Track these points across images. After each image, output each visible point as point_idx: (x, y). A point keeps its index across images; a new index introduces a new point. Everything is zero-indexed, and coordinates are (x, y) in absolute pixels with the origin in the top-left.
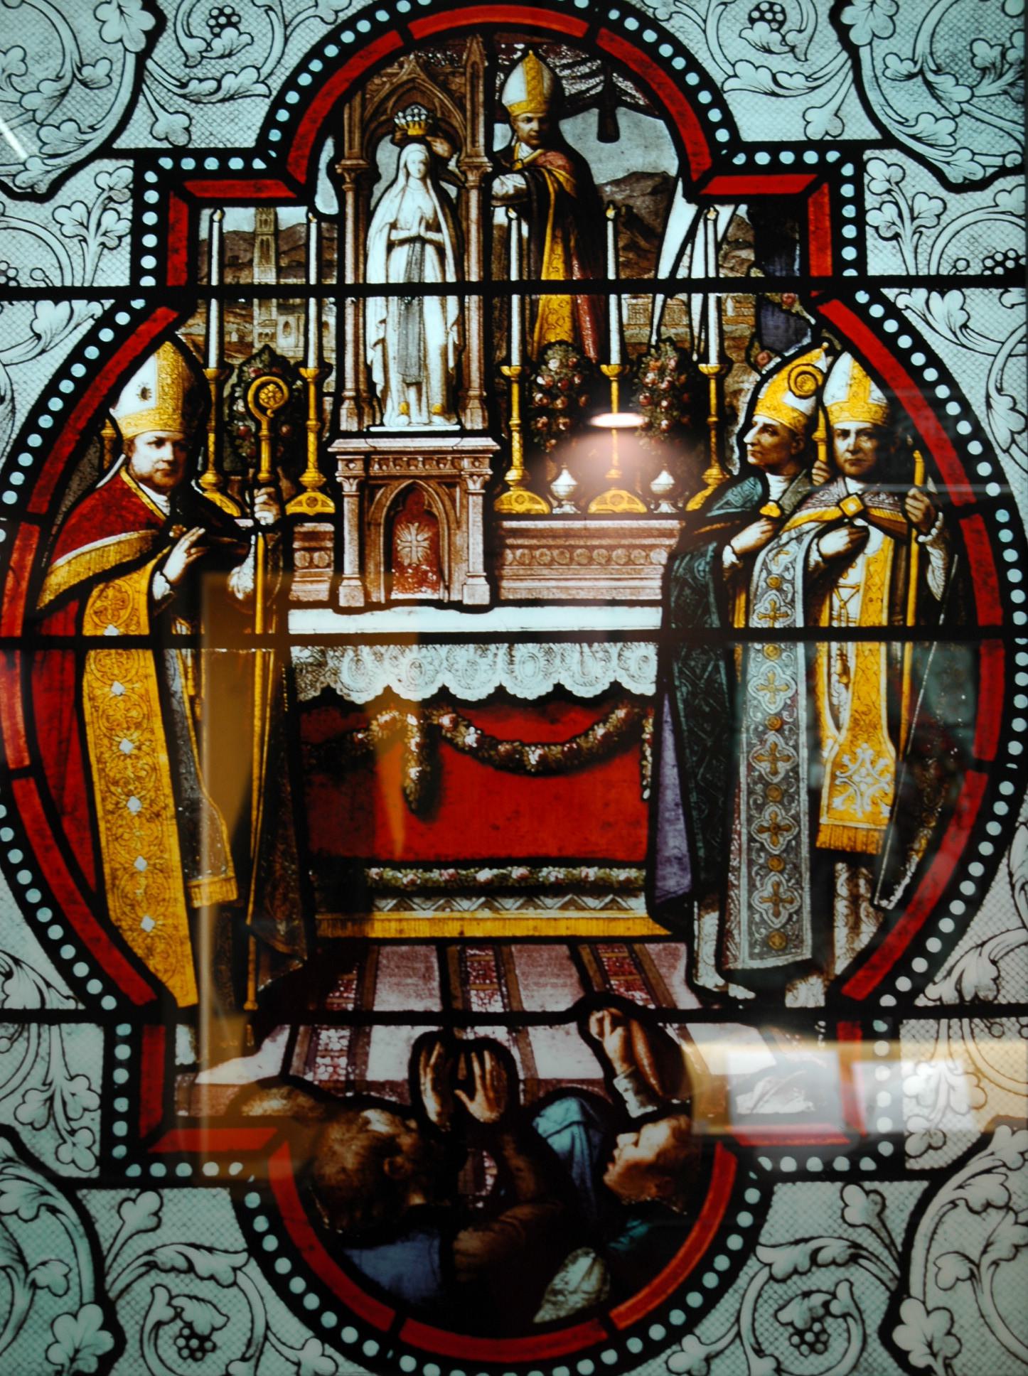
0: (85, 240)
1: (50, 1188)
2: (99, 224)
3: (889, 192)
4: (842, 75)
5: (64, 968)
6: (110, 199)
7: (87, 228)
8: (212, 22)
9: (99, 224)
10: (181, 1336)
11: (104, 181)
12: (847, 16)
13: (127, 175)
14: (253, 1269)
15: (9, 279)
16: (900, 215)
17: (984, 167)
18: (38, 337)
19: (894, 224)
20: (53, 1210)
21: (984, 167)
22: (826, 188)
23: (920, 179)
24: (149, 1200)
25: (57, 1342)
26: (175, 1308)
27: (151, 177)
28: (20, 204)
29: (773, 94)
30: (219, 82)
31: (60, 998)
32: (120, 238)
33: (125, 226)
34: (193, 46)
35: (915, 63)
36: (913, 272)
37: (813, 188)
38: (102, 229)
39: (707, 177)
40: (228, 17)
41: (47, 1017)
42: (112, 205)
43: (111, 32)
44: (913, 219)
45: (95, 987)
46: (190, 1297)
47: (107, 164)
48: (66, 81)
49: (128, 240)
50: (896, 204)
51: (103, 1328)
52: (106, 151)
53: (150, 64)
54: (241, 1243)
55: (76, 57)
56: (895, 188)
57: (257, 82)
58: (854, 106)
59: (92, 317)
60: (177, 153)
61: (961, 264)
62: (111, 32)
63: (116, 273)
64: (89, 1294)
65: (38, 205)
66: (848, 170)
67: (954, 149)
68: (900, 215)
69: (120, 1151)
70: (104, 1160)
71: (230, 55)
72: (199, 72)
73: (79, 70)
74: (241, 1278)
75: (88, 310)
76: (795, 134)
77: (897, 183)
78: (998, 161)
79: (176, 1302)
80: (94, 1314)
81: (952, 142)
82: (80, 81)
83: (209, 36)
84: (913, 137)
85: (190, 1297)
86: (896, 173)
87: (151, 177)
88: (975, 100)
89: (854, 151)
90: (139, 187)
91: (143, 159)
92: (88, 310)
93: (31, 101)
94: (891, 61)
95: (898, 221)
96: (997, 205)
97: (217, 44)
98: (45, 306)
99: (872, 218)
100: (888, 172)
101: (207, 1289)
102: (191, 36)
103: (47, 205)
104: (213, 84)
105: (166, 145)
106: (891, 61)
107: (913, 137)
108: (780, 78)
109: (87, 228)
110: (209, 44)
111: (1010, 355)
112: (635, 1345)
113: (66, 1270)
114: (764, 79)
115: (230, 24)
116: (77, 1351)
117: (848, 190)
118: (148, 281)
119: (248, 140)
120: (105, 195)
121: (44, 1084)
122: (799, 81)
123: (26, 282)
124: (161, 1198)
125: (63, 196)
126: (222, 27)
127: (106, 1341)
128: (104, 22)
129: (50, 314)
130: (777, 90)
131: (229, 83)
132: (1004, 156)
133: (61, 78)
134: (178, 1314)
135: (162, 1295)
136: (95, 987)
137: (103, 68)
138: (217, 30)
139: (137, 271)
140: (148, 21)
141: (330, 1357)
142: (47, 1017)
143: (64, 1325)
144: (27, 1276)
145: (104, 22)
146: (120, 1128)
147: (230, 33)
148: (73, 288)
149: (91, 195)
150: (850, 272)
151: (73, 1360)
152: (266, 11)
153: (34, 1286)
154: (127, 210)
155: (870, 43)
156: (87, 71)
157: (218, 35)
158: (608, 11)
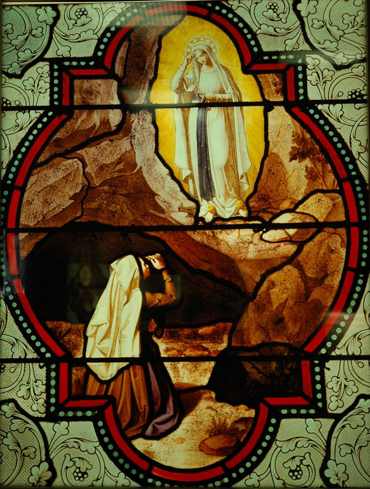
2: (38, 85)
3: (314, 68)
5: (32, 344)
7: (34, 87)
8: (77, 14)
9: (38, 85)
10: (75, 472)
11: (40, 70)
13: (47, 68)
14: (100, 448)
17: (348, 59)
20: (30, 429)
21: (348, 59)
24: (64, 424)
26: (73, 461)
30: (80, 35)
31: (32, 355)
32: (46, 90)
33: (48, 85)
35: (324, 22)
38: (39, 87)
39: (251, 64)
40: (83, 12)
41: (25, 361)
45: (43, 350)
46: (79, 458)
47: (41, 64)
49: (48, 91)
51: (49, 470)
52: (41, 58)
53: (55, 28)
56: (317, 67)
57: (93, 34)
61: (340, 94)
62: (41, 18)
64: (44, 458)
67: (337, 52)
71: (84, 25)
72: (73, 31)
73: (31, 31)
74: (97, 452)
75: (35, 115)
77: (317, 65)
78: (354, 57)
80: (45, 466)
83: (76, 19)
84: (323, 49)
85: (79, 458)
86: (317, 62)
87: (56, 67)
88: (345, 36)
90: (52, 70)
91: (52, 61)
92: (35, 115)
95: (318, 80)
96: (352, 72)
98: (20, 114)
100: (313, 62)
104: (77, 36)
105: (61, 57)
107: (323, 49)
108: (276, 29)
109: (34, 87)
110: (76, 21)
111: (358, 125)
112: (234, 475)
113: (34, 450)
115: (83, 14)
116: (40, 478)
120: (40, 75)
123: (13, 105)
126: (81, 15)
130: (276, 34)
131: (84, 36)
132: (356, 55)
133: (25, 34)
137: (40, 29)
138: (79, 16)
139: (52, 100)
142: (25, 361)
143: (35, 470)
144: (22, 452)
147: (84, 17)
148: (29, 106)
149: (35, 75)
151: (38, 482)
153: (24, 455)
154: (48, 80)
157: (80, 18)
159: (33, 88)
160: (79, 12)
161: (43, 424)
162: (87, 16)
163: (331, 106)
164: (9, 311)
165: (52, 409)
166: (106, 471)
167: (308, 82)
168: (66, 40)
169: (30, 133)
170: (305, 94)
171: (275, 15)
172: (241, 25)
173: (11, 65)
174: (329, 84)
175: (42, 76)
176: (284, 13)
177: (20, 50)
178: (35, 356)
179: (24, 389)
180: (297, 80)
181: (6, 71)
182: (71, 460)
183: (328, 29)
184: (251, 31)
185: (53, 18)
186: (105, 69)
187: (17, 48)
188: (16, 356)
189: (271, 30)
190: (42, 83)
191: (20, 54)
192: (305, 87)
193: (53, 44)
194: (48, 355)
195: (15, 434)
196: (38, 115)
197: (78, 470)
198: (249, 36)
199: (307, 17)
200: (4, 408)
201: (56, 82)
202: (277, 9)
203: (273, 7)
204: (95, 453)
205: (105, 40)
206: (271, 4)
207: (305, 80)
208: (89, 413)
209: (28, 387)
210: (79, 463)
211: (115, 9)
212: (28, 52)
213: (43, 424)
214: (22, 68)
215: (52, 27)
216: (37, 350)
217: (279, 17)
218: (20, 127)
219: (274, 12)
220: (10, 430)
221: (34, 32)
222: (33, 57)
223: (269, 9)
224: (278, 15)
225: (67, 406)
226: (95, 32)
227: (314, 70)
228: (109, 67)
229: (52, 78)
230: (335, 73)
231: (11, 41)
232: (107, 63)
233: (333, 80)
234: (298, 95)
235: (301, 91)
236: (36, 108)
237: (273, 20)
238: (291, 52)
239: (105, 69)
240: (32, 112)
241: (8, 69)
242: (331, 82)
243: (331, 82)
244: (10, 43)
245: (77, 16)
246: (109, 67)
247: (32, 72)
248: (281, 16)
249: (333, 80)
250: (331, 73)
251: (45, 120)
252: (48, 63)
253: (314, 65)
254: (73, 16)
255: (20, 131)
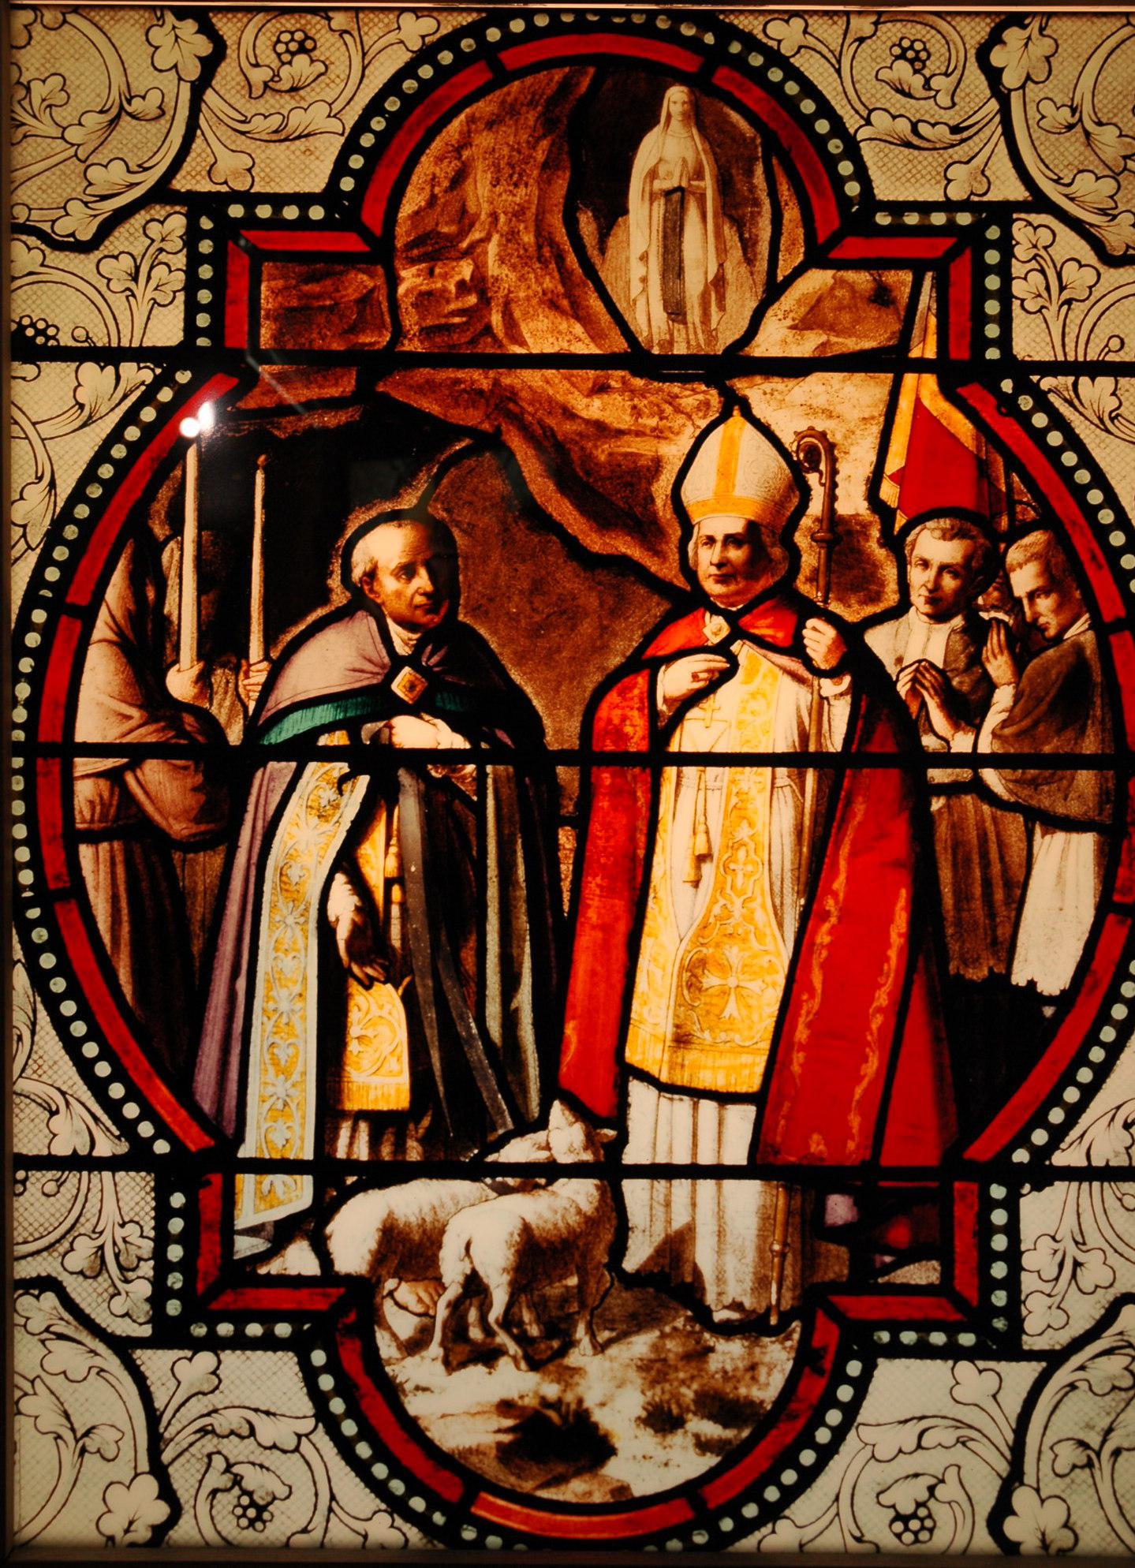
0: (133, 295)
1: (101, 1348)
3: (1034, 258)
4: (987, 132)
6: (161, 250)
12: (997, 58)
13: (177, 223)
15: (48, 338)
16: (1048, 288)
18: (82, 407)
19: (1039, 296)
22: (968, 255)
23: (1070, 244)
25: (109, 1511)
26: (236, 1475)
27: (206, 224)
28: (61, 255)
29: (908, 144)
34: (259, 76)
35: (1074, 111)
36: (1061, 358)
37: (953, 254)
38: (153, 284)
42: (163, 257)
43: (164, 60)
44: (1062, 288)
47: (159, 211)
48: (114, 111)
49: (181, 297)
50: (1043, 272)
53: (209, 96)
54: (308, 1408)
55: (124, 88)
58: (1002, 163)
59: (143, 383)
60: (235, 196)
61: (1115, 344)
62: (164, 60)
63: (167, 330)
65: (82, 256)
66: (993, 233)
68: (1048, 288)
69: (173, 1307)
70: (158, 1316)
73: (129, 102)
74: (305, 1446)
75: (136, 375)
76: (932, 193)
77: (1045, 248)
79: (235, 1469)
81: (1113, 205)
82: (129, 114)
83: (275, 64)
87: (206, 224)
89: (1003, 213)
90: (192, 236)
91: (196, 204)
93: (73, 134)
94: (1047, 108)
95: (1045, 294)
97: (285, 72)
98: (89, 368)
99: (1018, 288)
101: (272, 1459)
102: (257, 65)
103: (91, 256)
106: (1047, 108)
108: (923, 129)
114: (903, 127)
116: (131, 1523)
117: (992, 257)
118: (203, 342)
119: (317, 183)
120: (156, 245)
121: (94, 1232)
122: (943, 130)
123: (66, 340)
124: (219, 1362)
125: (113, 244)
127: (161, 1511)
128: (157, 48)
129: (95, 379)
130: (916, 141)
131: (298, 120)
134: (237, 1480)
135: (219, 1463)
136: (146, 1129)
137: (154, 98)
140: (205, 47)
141: (399, 1529)
145: (157, 48)
146: (175, 1280)
147: (301, 60)
149: (139, 246)
150: (993, 354)
151: (127, 1531)
152: (341, 36)
154: (180, 261)
155: (1023, 87)
156: (137, 105)
158: (729, 44)
159: (132, 285)
160: (287, 44)
161: (142, 1356)
162: (316, 54)
163: (1084, 381)
164: (40, 1007)
165: (173, 1307)
166: (334, 1504)
167: (1016, 304)
168: (243, 133)
169: (116, 436)
170: (1005, 341)
171: (918, 81)
172: (808, 107)
173: (64, 208)
174: (1078, 309)
175: (161, 250)
176: (947, 75)
177: (93, 159)
178: (123, 1148)
179: (84, 1248)
180: (981, 294)
181: (46, 227)
182: (229, 1467)
183: (1087, 134)
184: (838, 127)
185: (200, 58)
186: (365, 233)
187: (82, 154)
188: (61, 1149)
189: (903, 127)
190: (160, 272)
191: (93, 173)
192: (1005, 320)
193: (198, 144)
194: (162, 1147)
195: (57, 1383)
196: (147, 376)
197: (245, 1500)
198: (835, 146)
199: (1023, 87)
200: (25, 1303)
201: (206, 272)
202: (924, 62)
203: (910, 54)
204: (297, 1449)
205: (367, 140)
206: (906, 43)
207: (1005, 296)
208: (283, 1330)
209: (99, 1242)
210: (253, 1479)
211: (402, 36)
212: (118, 167)
213: (142, 1356)
214: (100, 219)
215: (199, 88)
216: (127, 1128)
217: (930, 89)
218: (86, 412)
219: (916, 72)
220: (39, 1371)
221: (137, 105)
222: (132, 186)
223: (897, 58)
224: (927, 81)
225: (215, 1306)
226: (336, 107)
227: (1034, 265)
228: (377, 230)
229: (195, 261)
230: (1099, 275)
231: (64, 129)
232: (372, 215)
233: (1093, 299)
234: (982, 343)
235: (992, 331)
236: (141, 355)
237: (909, 95)
238: (965, 205)
239: (365, 233)
240: (128, 369)
241: (54, 222)
242: (1088, 303)
243: (1088, 303)
244: (63, 138)
245: (279, 55)
246: (377, 230)
247: (127, 238)
248: (935, 83)
249: (1093, 299)
250: (1089, 276)
251: (165, 395)
252: (184, 210)
253: (1035, 246)
254: (267, 57)
255: (84, 425)
